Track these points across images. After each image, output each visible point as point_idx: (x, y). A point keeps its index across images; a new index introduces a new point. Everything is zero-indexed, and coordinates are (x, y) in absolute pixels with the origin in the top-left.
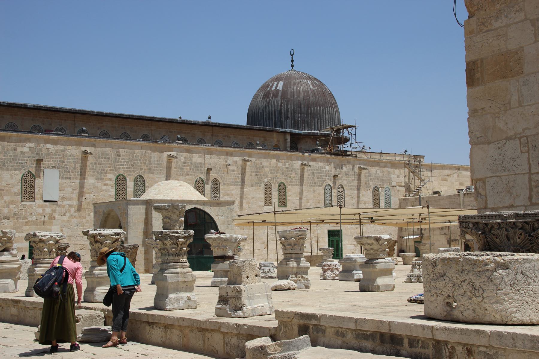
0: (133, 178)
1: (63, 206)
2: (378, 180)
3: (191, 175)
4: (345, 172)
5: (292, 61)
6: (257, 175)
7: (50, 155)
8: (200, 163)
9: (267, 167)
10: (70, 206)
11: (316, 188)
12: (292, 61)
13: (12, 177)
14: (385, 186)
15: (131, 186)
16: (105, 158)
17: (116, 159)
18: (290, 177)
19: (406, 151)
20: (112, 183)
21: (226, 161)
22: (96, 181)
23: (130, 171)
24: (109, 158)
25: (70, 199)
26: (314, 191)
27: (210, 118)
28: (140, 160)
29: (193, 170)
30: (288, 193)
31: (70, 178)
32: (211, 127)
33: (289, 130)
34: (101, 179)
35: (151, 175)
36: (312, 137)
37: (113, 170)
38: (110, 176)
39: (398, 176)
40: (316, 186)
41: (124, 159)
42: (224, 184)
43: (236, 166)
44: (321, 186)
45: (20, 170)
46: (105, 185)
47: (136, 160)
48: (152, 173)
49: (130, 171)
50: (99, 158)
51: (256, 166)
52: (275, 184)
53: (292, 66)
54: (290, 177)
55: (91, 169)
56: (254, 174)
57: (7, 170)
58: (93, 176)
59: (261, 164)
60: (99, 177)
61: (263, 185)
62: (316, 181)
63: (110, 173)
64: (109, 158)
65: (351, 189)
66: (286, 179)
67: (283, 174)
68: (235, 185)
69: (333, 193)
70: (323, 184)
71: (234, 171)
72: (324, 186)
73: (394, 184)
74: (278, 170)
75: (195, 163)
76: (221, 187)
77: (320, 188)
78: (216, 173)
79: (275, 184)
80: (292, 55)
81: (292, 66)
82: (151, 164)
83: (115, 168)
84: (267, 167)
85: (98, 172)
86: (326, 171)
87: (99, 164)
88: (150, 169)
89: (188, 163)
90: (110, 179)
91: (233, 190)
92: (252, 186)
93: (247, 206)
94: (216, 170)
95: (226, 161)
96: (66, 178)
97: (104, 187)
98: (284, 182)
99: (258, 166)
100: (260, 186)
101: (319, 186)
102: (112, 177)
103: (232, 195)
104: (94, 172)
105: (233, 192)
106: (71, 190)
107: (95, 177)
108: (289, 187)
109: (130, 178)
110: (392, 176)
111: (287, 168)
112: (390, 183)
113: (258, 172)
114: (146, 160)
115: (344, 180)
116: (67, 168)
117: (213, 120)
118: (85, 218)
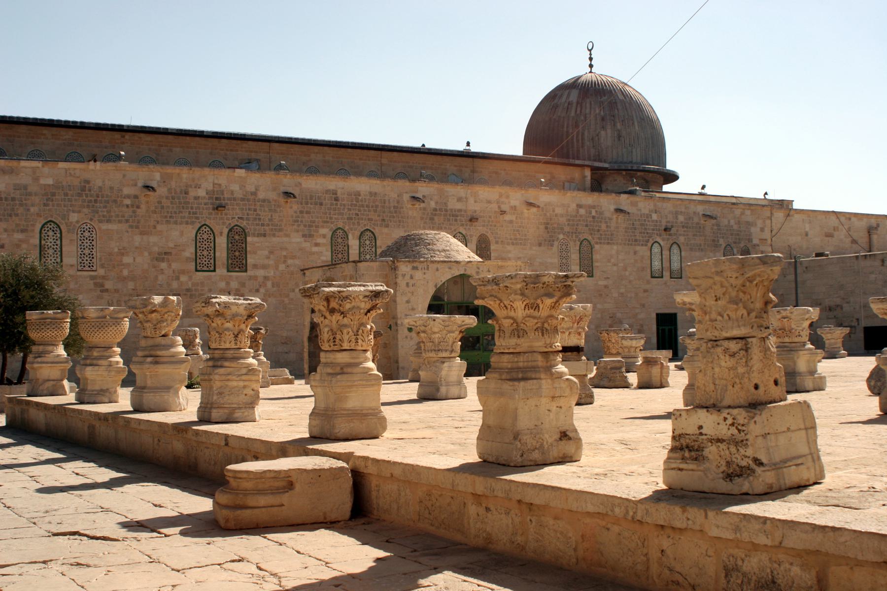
0: (358, 233)
1: (255, 278)
2: (732, 235)
5: (591, 59)
6: (546, 228)
7: (235, 199)
8: (460, 210)
10: (266, 278)
11: (638, 248)
12: (591, 59)
13: (182, 234)
14: (742, 245)
15: (354, 247)
16: (316, 204)
17: (332, 204)
18: (598, 231)
19: (766, 194)
20: (326, 241)
21: (499, 207)
22: (302, 239)
23: (354, 224)
24: (321, 204)
25: (264, 267)
26: (635, 253)
27: (468, 144)
28: (368, 206)
29: (449, 220)
30: (596, 257)
31: (265, 235)
32: (471, 159)
33: (587, 163)
34: (311, 236)
35: (385, 230)
36: (624, 173)
37: (328, 222)
38: (323, 231)
39: (762, 230)
41: (344, 205)
42: (497, 243)
44: (646, 245)
45: (193, 223)
46: (317, 245)
47: (363, 206)
48: (387, 226)
49: (354, 224)
50: (307, 203)
51: (545, 215)
52: (575, 241)
53: (591, 66)
54: (598, 231)
55: (295, 221)
56: (542, 227)
57: (176, 223)
58: (298, 231)
59: (554, 211)
60: (306, 232)
63: (323, 227)
64: (321, 204)
65: (691, 249)
66: (591, 234)
67: (587, 226)
68: (513, 244)
70: (648, 241)
71: (511, 222)
72: (650, 245)
73: (755, 241)
75: (451, 210)
76: (493, 247)
78: (484, 226)
80: (590, 50)
81: (591, 66)
82: (384, 212)
83: (331, 218)
85: (305, 226)
86: (653, 221)
87: (308, 212)
88: (383, 220)
89: (440, 210)
90: (324, 236)
91: (510, 252)
92: (540, 245)
95: (499, 207)
96: (259, 235)
97: (315, 249)
98: (590, 238)
99: (548, 214)
100: (552, 245)
102: (326, 231)
104: (299, 226)
105: (510, 255)
106: (266, 253)
107: (301, 233)
108: (597, 247)
109: (353, 234)
110: (753, 229)
111: (594, 217)
112: (750, 240)
114: (377, 206)
116: (260, 219)
117: (474, 149)
118: (288, 296)
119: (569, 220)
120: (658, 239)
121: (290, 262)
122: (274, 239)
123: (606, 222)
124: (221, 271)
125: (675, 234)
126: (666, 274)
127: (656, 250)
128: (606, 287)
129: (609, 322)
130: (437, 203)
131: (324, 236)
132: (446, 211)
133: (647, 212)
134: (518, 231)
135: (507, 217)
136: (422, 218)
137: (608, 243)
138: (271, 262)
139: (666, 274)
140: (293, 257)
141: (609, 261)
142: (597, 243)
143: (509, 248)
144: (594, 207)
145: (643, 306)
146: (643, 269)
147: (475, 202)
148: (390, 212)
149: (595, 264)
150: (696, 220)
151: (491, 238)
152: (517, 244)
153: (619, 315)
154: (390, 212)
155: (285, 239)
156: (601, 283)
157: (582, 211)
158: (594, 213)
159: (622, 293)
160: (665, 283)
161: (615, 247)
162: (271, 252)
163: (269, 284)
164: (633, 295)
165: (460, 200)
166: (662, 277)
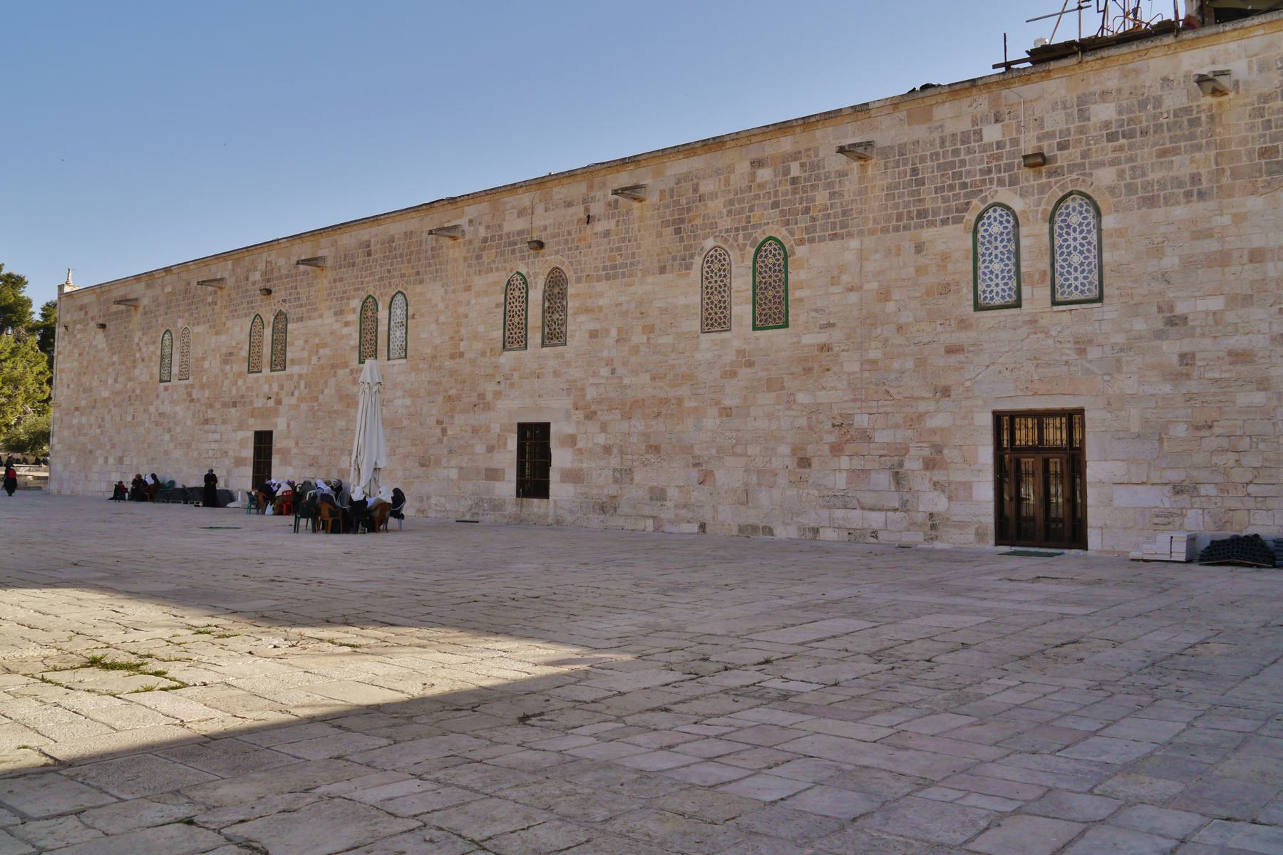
3: (497, 269)
4: (1107, 124)
9: (714, 195)
11: (927, 234)
18: (807, 210)
20: (354, 317)
21: (587, 210)
26: (919, 248)
29: (503, 254)
35: (419, 289)
40: (932, 224)
42: (579, 280)
43: (613, 216)
44: (958, 220)
48: (421, 282)
52: (742, 248)
54: (807, 210)
59: (696, 190)
61: (698, 261)
62: (928, 205)
65: (1150, 202)
66: (787, 223)
67: (775, 205)
68: (608, 278)
69: (1024, 242)
71: (607, 234)
72: (971, 217)
74: (757, 197)
77: (950, 229)
78: (557, 252)
79: (742, 248)
84: (714, 195)
87: (341, 280)
88: (418, 273)
91: (601, 295)
92: (662, 270)
93: (645, 338)
94: (558, 243)
98: (782, 234)
99: (683, 201)
100: (688, 267)
101: (944, 222)
102: (356, 303)
103: (600, 309)
105: (601, 302)
108: (801, 251)
111: (794, 181)
113: (682, 221)
115: (1101, 164)
119: (731, 202)
120: (1005, 195)
121: (322, 351)
122: (310, 323)
123: (829, 185)
124: (266, 370)
125: (1072, 168)
126: (1036, 296)
127: (996, 229)
128: (824, 348)
129: (831, 438)
130: (488, 227)
131: (354, 310)
132: (501, 237)
133: (965, 125)
134: (619, 249)
135: (600, 227)
136: (465, 259)
137: (834, 237)
138: (305, 355)
139: (1036, 296)
140: (325, 345)
141: (835, 281)
142: (801, 242)
143: (600, 286)
144: (795, 156)
145: (946, 392)
146: (945, 289)
147: (546, 211)
148: (426, 258)
149: (794, 294)
150: (1174, 100)
151: (570, 274)
152: (615, 277)
153: (862, 420)
154: (426, 258)
155: (319, 321)
156: (808, 339)
157: (765, 174)
158: (795, 170)
159: (874, 362)
160: (1033, 322)
161: (854, 243)
162: (306, 341)
163: (302, 384)
164: (910, 364)
165: (521, 213)
166: (1018, 304)
